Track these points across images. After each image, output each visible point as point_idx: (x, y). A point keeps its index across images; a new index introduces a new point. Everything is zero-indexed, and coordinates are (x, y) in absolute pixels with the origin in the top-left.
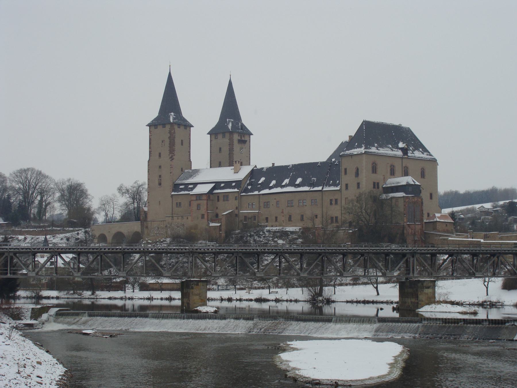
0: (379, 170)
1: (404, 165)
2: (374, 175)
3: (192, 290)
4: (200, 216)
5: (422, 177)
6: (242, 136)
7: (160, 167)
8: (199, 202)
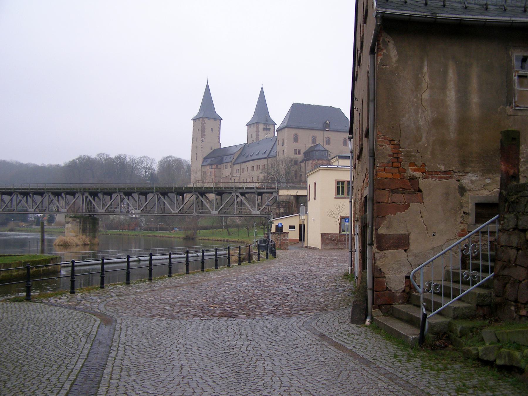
0: (299, 140)
1: (326, 136)
2: (295, 144)
5: (344, 145)
6: (267, 126)
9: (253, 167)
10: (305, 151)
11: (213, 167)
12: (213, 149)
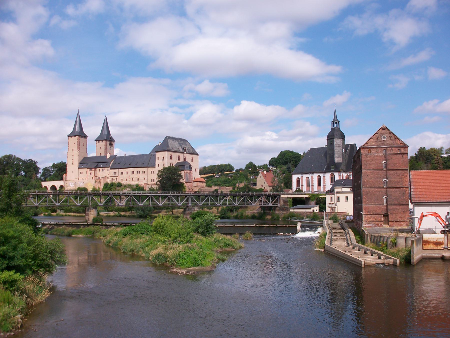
2: (171, 160)
3: (90, 212)
4: (92, 178)
7: (73, 155)
8: (91, 172)
9: (133, 173)
10: (175, 164)
11: (93, 169)
12: (84, 157)
